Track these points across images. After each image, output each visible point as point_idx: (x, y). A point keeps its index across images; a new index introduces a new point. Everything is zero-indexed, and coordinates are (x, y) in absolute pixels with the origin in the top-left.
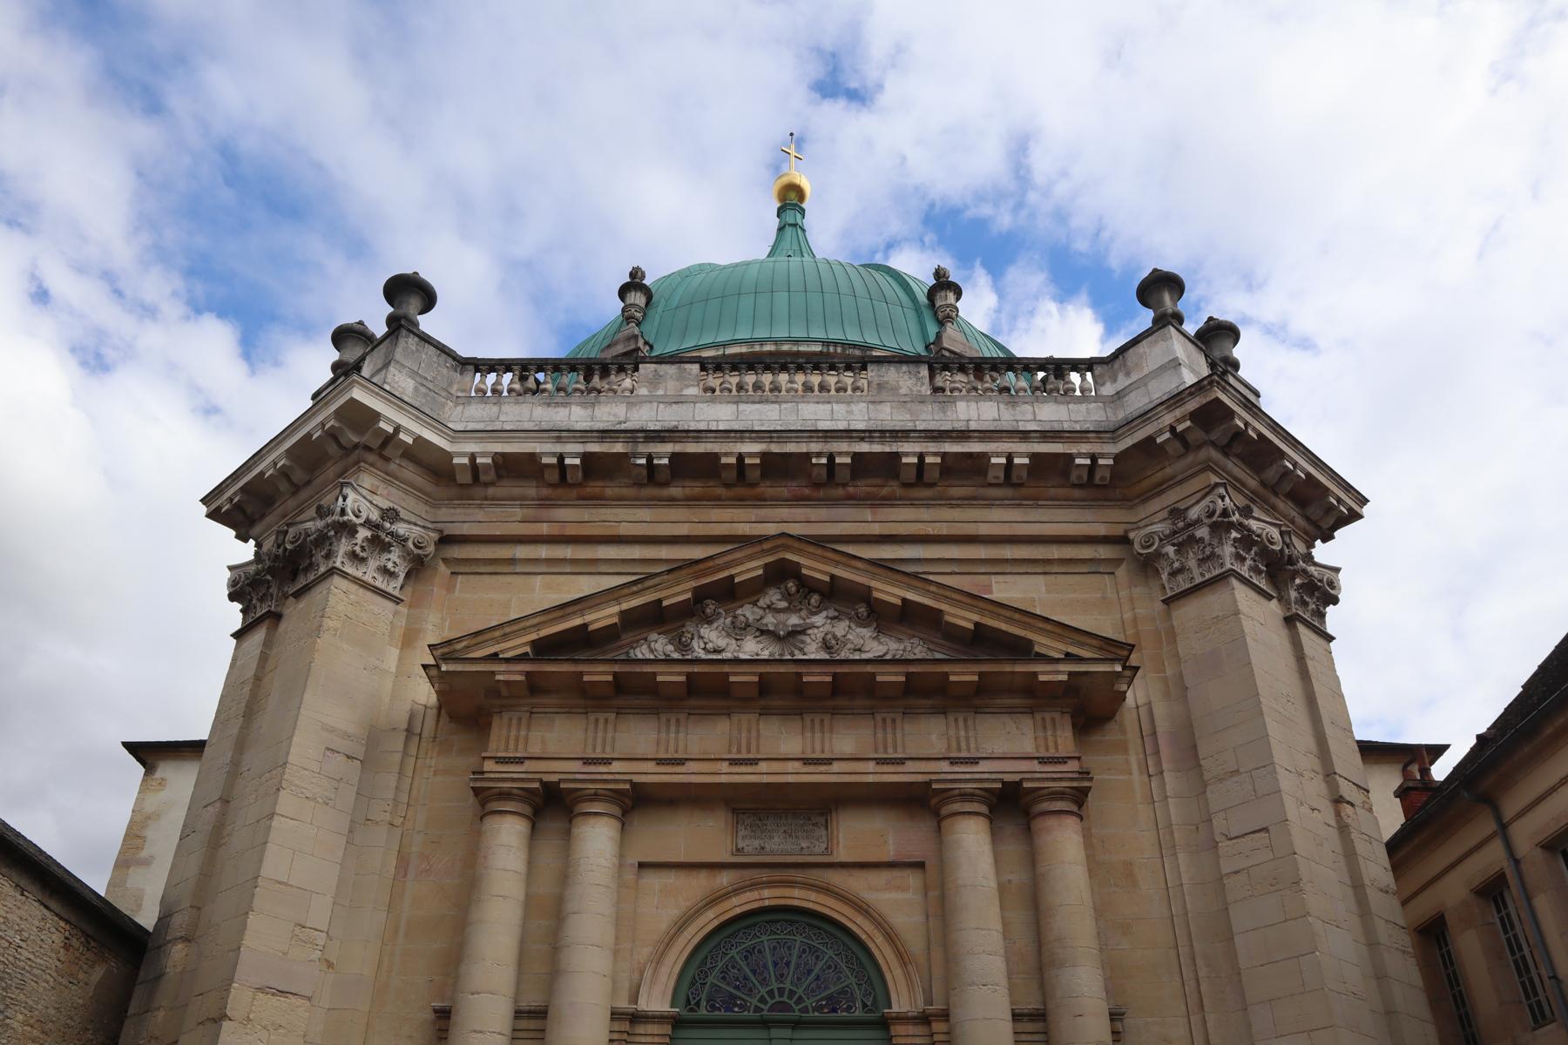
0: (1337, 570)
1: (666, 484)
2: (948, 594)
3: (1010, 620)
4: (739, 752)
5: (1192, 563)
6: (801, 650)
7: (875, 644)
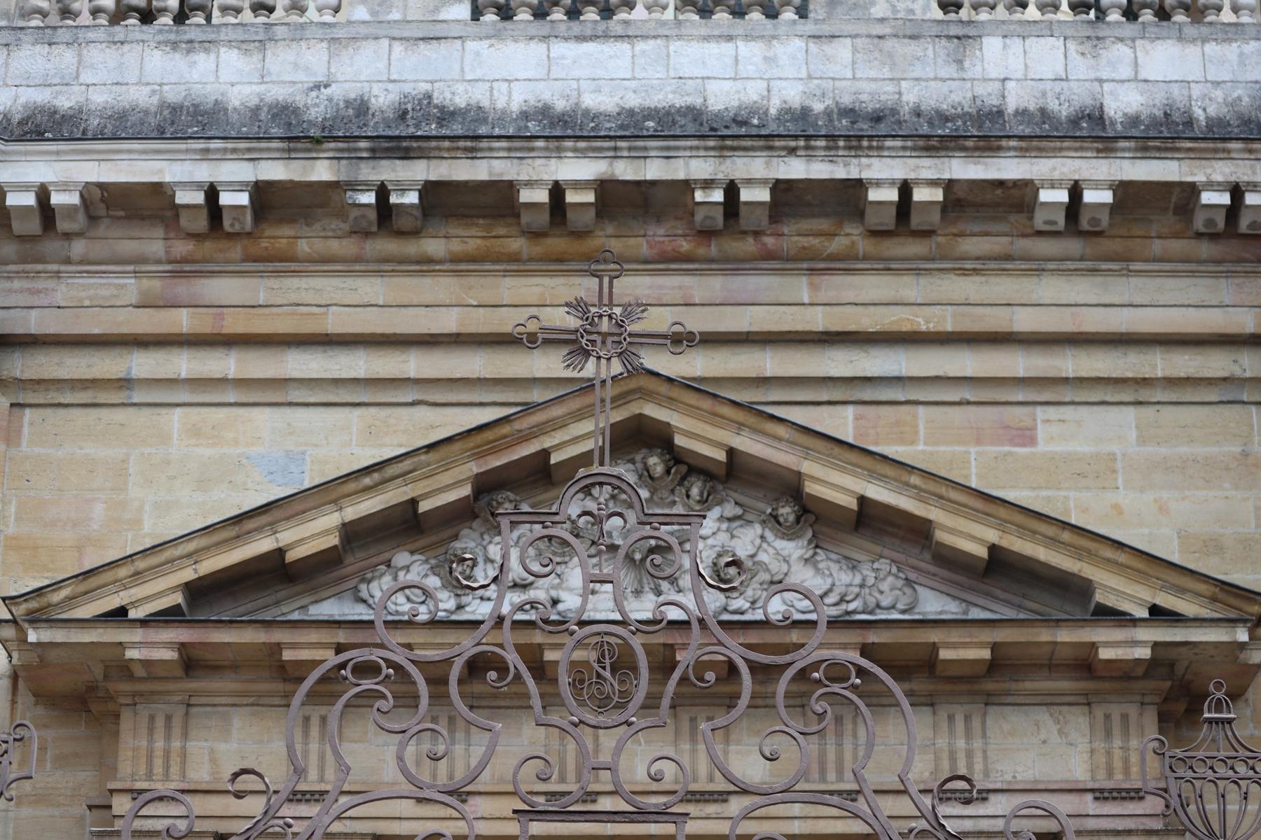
1: (415, 233)
2: (943, 490)
3: (1053, 542)
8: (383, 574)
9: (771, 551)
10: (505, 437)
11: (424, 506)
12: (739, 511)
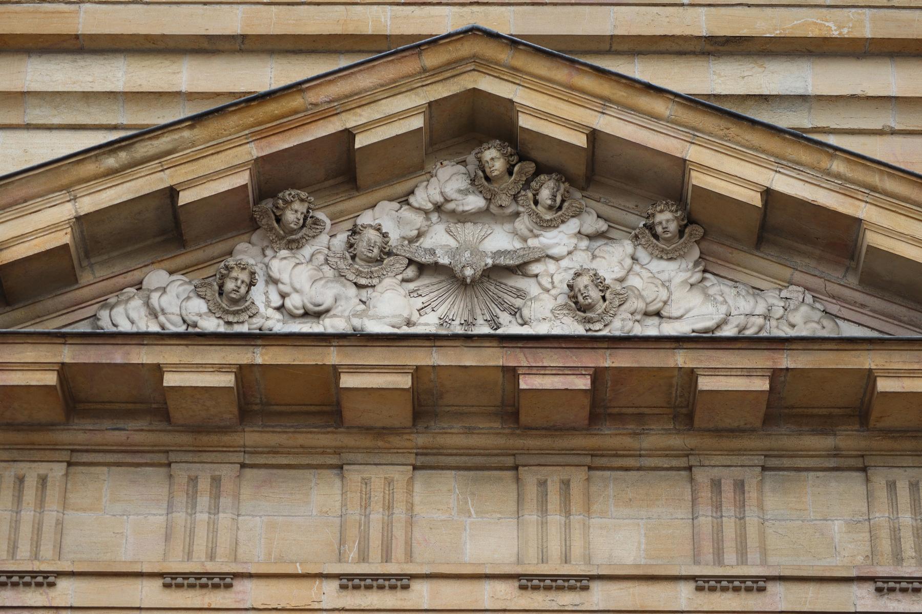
4: (363, 557)
6: (515, 312)
8: (130, 299)
9: (645, 274)
10: (296, 112)
11: (185, 198)
12: (602, 226)
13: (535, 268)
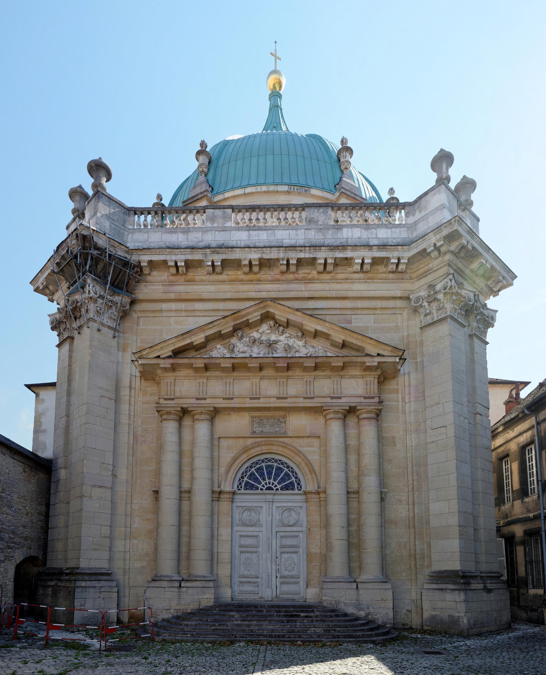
0: (496, 311)
5: (434, 311)
7: (304, 348)
13: (279, 343)
